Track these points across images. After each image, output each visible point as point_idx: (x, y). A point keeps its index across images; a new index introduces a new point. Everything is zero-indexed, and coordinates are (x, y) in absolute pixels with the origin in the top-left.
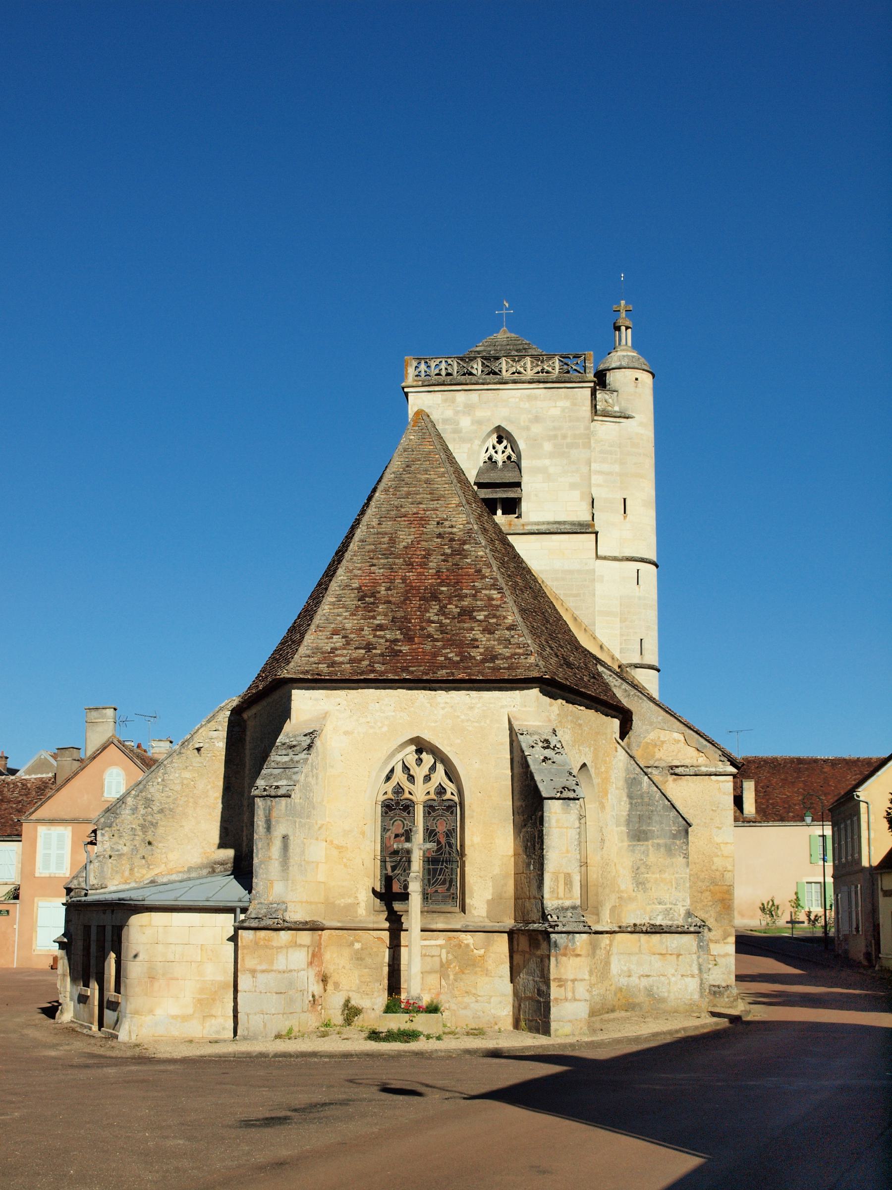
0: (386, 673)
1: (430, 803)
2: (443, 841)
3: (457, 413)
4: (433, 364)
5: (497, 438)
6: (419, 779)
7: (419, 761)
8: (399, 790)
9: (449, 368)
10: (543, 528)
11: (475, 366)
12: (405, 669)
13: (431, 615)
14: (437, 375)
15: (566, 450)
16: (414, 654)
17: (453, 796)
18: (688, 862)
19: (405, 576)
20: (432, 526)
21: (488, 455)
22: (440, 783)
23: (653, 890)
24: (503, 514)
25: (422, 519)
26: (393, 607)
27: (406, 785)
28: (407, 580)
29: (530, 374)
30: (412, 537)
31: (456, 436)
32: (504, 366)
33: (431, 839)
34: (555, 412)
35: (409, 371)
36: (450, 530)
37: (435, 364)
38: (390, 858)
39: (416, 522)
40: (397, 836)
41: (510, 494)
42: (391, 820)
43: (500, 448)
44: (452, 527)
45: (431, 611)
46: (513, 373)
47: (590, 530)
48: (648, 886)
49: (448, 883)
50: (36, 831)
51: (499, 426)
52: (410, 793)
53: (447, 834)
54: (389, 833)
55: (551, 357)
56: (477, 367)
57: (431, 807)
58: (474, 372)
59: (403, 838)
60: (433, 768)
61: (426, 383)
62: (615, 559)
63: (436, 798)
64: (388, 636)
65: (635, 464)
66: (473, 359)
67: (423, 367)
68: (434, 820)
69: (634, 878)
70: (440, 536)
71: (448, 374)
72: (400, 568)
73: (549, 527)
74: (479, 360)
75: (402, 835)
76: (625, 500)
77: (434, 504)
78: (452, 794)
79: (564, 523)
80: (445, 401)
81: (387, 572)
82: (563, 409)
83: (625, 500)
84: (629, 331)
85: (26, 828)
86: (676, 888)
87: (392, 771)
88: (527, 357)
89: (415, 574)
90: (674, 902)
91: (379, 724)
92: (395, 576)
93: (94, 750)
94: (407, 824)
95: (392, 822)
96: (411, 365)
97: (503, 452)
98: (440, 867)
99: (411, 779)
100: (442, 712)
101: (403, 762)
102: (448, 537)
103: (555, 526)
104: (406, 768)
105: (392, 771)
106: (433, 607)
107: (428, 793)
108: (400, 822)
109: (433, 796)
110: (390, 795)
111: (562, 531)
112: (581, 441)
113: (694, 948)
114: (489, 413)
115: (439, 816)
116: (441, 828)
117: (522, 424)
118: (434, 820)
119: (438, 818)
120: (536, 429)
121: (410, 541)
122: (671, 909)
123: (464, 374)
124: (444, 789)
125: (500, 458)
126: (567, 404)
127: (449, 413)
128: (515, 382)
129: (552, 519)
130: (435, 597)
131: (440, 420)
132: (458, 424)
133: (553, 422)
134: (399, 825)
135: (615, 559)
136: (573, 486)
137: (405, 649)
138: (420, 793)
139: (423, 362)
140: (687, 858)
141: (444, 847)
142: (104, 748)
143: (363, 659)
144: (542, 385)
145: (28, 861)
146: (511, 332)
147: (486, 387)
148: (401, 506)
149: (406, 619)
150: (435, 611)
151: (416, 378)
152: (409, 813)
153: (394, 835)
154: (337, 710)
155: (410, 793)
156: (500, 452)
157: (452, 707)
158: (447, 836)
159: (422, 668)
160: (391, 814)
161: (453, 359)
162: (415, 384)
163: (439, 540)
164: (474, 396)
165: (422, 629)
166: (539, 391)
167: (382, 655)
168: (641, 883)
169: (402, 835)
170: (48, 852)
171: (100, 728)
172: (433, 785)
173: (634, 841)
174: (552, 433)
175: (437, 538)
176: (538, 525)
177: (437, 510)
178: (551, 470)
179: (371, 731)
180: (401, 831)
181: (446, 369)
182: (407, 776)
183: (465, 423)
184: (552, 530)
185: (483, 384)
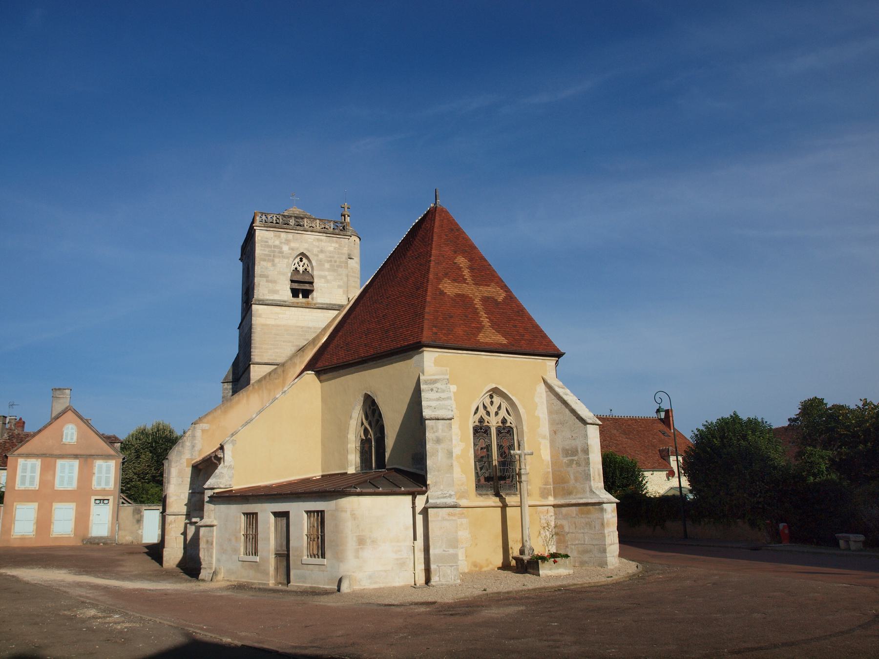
2: (507, 451)
3: (281, 243)
4: (269, 217)
6: (492, 414)
7: (492, 403)
8: (481, 420)
11: (291, 221)
14: (271, 222)
15: (336, 268)
21: (295, 266)
24: (303, 298)
27: (486, 417)
31: (281, 255)
34: (332, 249)
38: (478, 462)
41: (307, 287)
42: (478, 438)
43: (301, 264)
46: (310, 227)
50: (17, 462)
52: (488, 422)
54: (477, 447)
55: (330, 221)
56: (292, 222)
58: (291, 224)
59: (485, 450)
60: (499, 408)
61: (266, 226)
66: (290, 217)
67: (264, 217)
71: (277, 223)
74: (293, 218)
75: (485, 448)
78: (511, 423)
80: (275, 236)
82: (335, 249)
85: (10, 460)
87: (477, 409)
93: (57, 413)
96: (258, 216)
97: (303, 266)
99: (488, 413)
101: (483, 404)
104: (485, 407)
109: (500, 424)
110: (477, 423)
112: (343, 265)
114: (298, 245)
116: (506, 444)
117: (314, 253)
120: (321, 256)
123: (285, 224)
124: (506, 420)
125: (301, 269)
126: (337, 246)
127: (277, 243)
128: (312, 231)
133: (330, 253)
134: (483, 442)
136: (339, 287)
138: (494, 422)
139: (264, 215)
142: (64, 412)
144: (325, 235)
145: (12, 479)
147: (297, 232)
151: (261, 223)
152: (487, 434)
153: (480, 449)
155: (488, 422)
158: (509, 449)
162: (260, 225)
164: (290, 236)
166: (323, 237)
169: (485, 448)
170: (24, 474)
171: (62, 401)
174: (329, 259)
178: (329, 278)
180: (484, 446)
181: (276, 220)
183: (285, 248)
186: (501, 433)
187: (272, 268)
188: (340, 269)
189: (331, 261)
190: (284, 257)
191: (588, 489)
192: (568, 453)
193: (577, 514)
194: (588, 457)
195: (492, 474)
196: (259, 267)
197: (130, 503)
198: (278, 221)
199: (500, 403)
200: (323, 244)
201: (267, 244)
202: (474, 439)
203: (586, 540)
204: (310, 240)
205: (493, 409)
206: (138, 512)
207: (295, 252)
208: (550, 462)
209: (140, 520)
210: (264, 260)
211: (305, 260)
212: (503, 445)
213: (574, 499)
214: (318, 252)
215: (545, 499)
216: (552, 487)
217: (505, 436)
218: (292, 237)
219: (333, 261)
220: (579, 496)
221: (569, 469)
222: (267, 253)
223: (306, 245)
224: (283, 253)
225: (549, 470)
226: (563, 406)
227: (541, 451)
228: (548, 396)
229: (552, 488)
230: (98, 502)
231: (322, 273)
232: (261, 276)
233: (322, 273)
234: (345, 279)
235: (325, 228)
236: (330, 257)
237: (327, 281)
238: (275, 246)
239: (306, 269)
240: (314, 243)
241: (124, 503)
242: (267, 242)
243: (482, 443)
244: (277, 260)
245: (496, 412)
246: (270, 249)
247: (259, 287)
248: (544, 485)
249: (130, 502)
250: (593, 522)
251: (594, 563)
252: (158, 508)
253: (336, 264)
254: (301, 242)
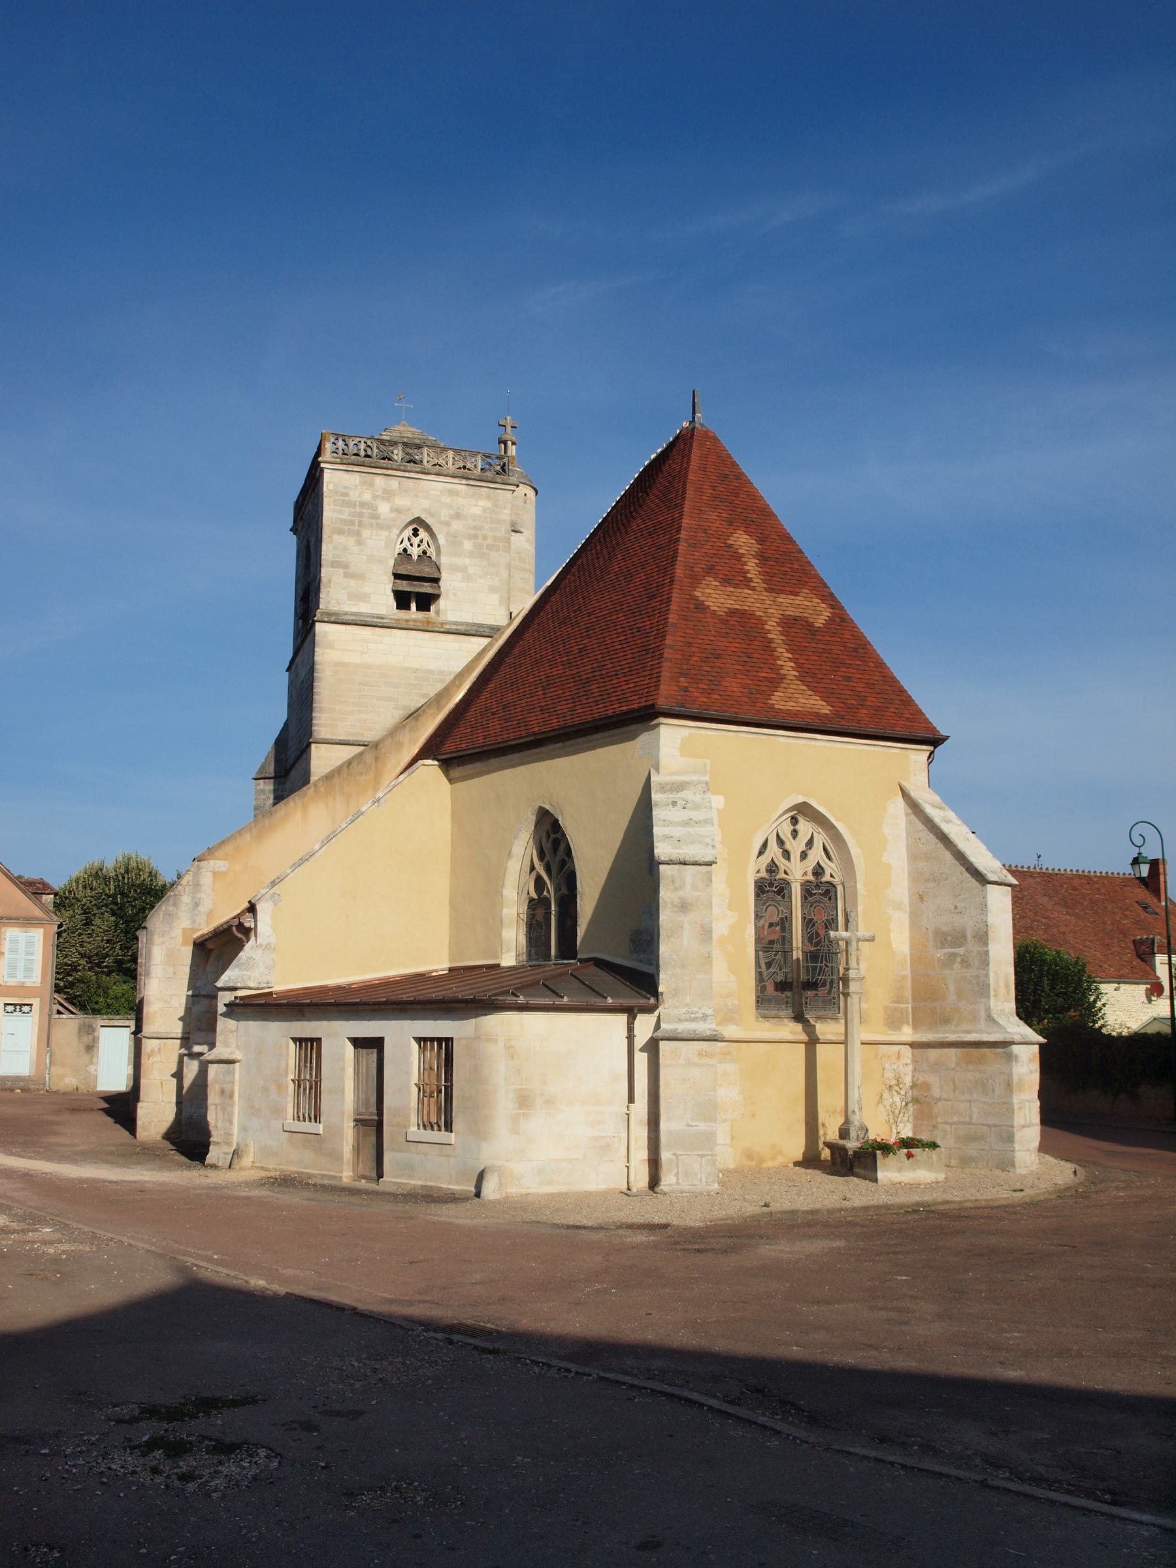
2: (822, 932)
3: (375, 497)
4: (351, 444)
5: (413, 530)
7: (795, 833)
8: (772, 868)
9: (369, 450)
10: (462, 628)
11: (395, 452)
15: (485, 551)
17: (832, 879)
22: (818, 863)
27: (782, 863)
29: (451, 468)
31: (374, 521)
33: (809, 931)
34: (477, 511)
35: (326, 446)
37: (354, 442)
40: (771, 925)
41: (426, 588)
42: (763, 905)
46: (435, 465)
51: (419, 518)
52: (786, 873)
53: (825, 924)
54: (762, 921)
55: (476, 454)
56: (398, 454)
58: (396, 458)
59: (778, 928)
60: (810, 843)
61: (345, 461)
65: (522, 579)
67: (340, 444)
68: (811, 907)
71: (367, 456)
74: (400, 447)
75: (777, 924)
78: (832, 876)
80: (363, 483)
82: (484, 510)
84: (514, 446)
87: (765, 845)
88: (450, 451)
94: (782, 911)
95: (765, 907)
96: (329, 440)
97: (419, 546)
98: (819, 965)
99: (787, 855)
101: (778, 835)
104: (780, 842)
108: (774, 908)
109: (810, 877)
110: (764, 874)
112: (501, 544)
115: (816, 902)
116: (820, 918)
117: (443, 518)
118: (811, 907)
119: (816, 904)
120: (457, 526)
123: (384, 459)
124: (822, 868)
125: (415, 552)
126: (489, 504)
127: (367, 497)
131: (358, 503)
132: (376, 509)
133: (474, 520)
136: (492, 589)
138: (797, 873)
139: (340, 439)
141: (823, 940)
144: (464, 482)
146: (411, 426)
147: (407, 474)
151: (335, 454)
152: (783, 897)
155: (786, 873)
156: (415, 545)
158: (827, 927)
161: (372, 441)
162: (332, 460)
164: (394, 483)
166: (460, 486)
169: (777, 924)
172: (811, 863)
174: (472, 532)
176: (457, 625)
178: (471, 570)
180: (776, 919)
181: (365, 451)
183: (384, 508)
184: (471, 632)
185: (404, 471)
186: (811, 895)
187: (356, 549)
188: (493, 554)
189: (476, 537)
190: (381, 527)
191: (983, 1014)
192: (946, 939)
193: (958, 1064)
194: (986, 949)
195: (789, 976)
196: (331, 546)
197: (73, 1013)
198: (369, 453)
199: (812, 835)
200: (460, 500)
201: (347, 498)
202: (756, 906)
203: (975, 1116)
204: (434, 492)
205: (796, 847)
206: (89, 1030)
208: (908, 957)
209: (93, 1046)
210: (341, 532)
211: (422, 534)
212: (815, 919)
213: (954, 1032)
214: (451, 517)
215: (893, 1030)
216: (910, 1006)
217: (820, 902)
218: (397, 485)
219: (480, 537)
220: (964, 1027)
221: (946, 972)
222: (345, 517)
223: (426, 503)
224: (379, 518)
225: (905, 973)
226: (940, 845)
227: (892, 935)
228: (909, 822)
229: (910, 1009)
230: (10, 1008)
231: (458, 561)
232: (335, 564)
233: (458, 561)
234: (504, 574)
235: (464, 467)
236: (475, 528)
237: (468, 578)
238: (363, 504)
239: (424, 552)
240: (443, 499)
241: (62, 1013)
242: (346, 495)
243: (772, 915)
244: (366, 533)
245: (802, 852)
246: (352, 510)
247: (330, 587)
248: (894, 1002)
249: (74, 1011)
250: (990, 1080)
251: (987, 1162)
252: (127, 1023)
253: (485, 542)
254: (416, 496)
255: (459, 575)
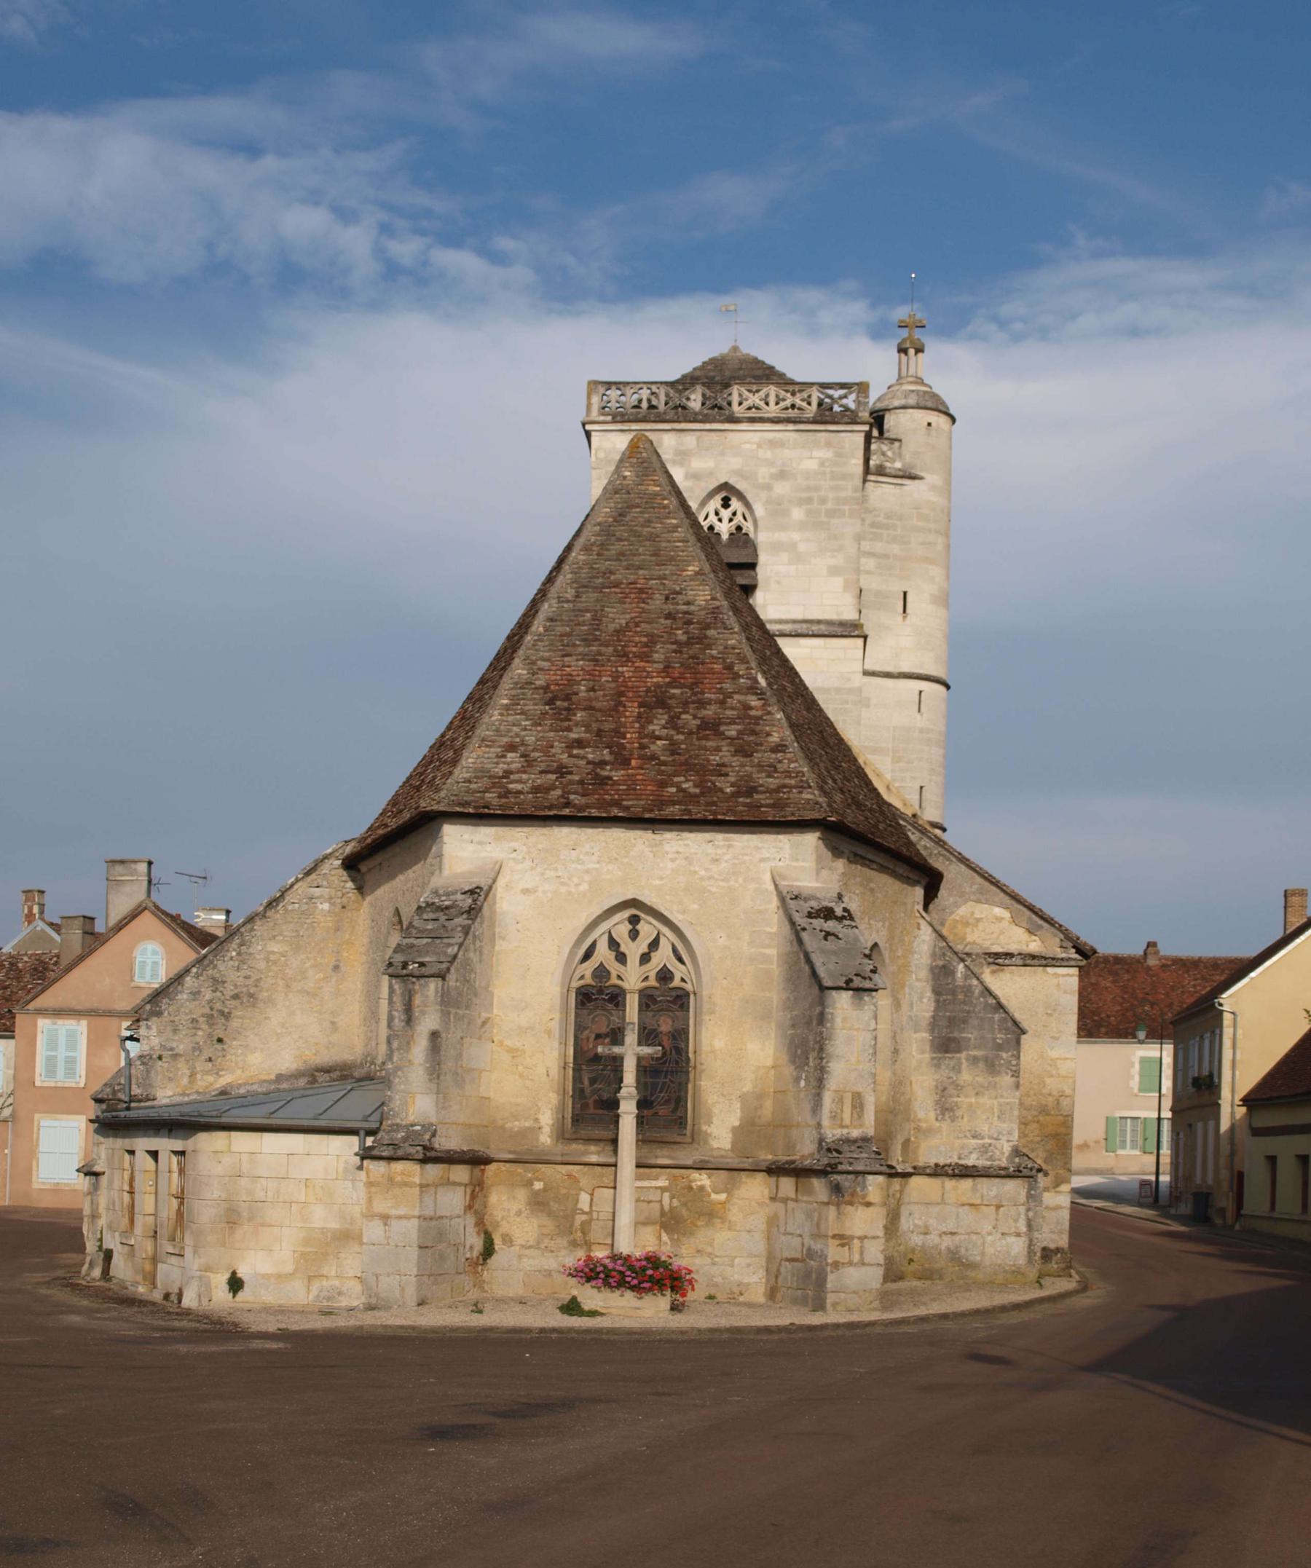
0: (588, 807)
1: (649, 992)
5: (723, 499)
6: (634, 959)
7: (634, 935)
8: (601, 972)
12: (617, 804)
13: (655, 727)
15: (825, 520)
16: (629, 783)
18: (1018, 1082)
19: (617, 671)
20: (658, 602)
23: (965, 1119)
25: (641, 591)
26: (599, 715)
27: (614, 967)
28: (619, 677)
29: (773, 410)
30: (628, 616)
32: (735, 399)
34: (811, 465)
36: (684, 608)
39: (633, 596)
40: (598, 1036)
44: (688, 603)
45: (655, 721)
46: (749, 408)
47: (856, 633)
48: (958, 1113)
49: (672, 1106)
52: (619, 977)
57: (651, 998)
59: (607, 1040)
60: (654, 945)
62: (888, 675)
63: (657, 985)
64: (590, 756)
65: (922, 544)
69: (937, 1102)
70: (669, 616)
72: (609, 660)
73: (797, 627)
75: (607, 1035)
76: (905, 594)
77: (658, 571)
79: (819, 622)
81: (589, 666)
82: (822, 463)
83: (905, 594)
86: (999, 1117)
87: (593, 945)
89: (632, 669)
90: (995, 1136)
91: (576, 880)
92: (600, 671)
97: (731, 520)
99: (622, 958)
100: (670, 865)
101: (610, 933)
102: (680, 618)
103: (804, 626)
104: (613, 944)
105: (593, 945)
106: (659, 716)
107: (646, 978)
109: (653, 982)
111: (816, 633)
112: (847, 508)
113: (1023, 1198)
120: (781, 489)
121: (623, 622)
122: (990, 1145)
126: (828, 454)
128: (752, 420)
129: (800, 616)
130: (662, 703)
133: (807, 479)
135: (888, 675)
136: (834, 571)
137: (617, 775)
138: (633, 978)
140: (1018, 1077)
143: (553, 787)
144: (791, 427)
147: (708, 426)
148: (611, 573)
149: (619, 732)
150: (664, 722)
152: (617, 1005)
154: (513, 859)
156: (725, 520)
157: (686, 858)
159: (643, 803)
160: (590, 1005)
163: (669, 622)
165: (642, 747)
166: (787, 434)
167: (581, 782)
168: (947, 1109)
173: (940, 1052)
174: (804, 495)
175: (666, 618)
177: (665, 579)
178: (802, 548)
179: (563, 889)
180: (604, 1030)
182: (614, 953)
188: (835, 521)
189: (809, 500)
198: (654, 402)
200: (787, 453)
204: (747, 446)
205: (634, 950)
207: (703, 484)
211: (735, 504)
214: (772, 476)
218: (694, 442)
219: (816, 499)
223: (735, 462)
231: (782, 536)
233: (782, 536)
235: (793, 406)
236: (808, 489)
237: (798, 558)
239: (739, 528)
240: (761, 453)
253: (823, 507)
254: (722, 454)
255: (785, 556)
